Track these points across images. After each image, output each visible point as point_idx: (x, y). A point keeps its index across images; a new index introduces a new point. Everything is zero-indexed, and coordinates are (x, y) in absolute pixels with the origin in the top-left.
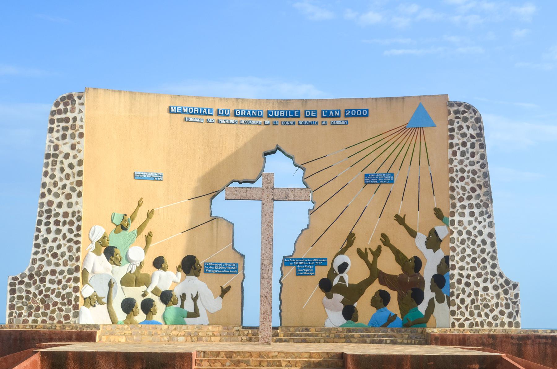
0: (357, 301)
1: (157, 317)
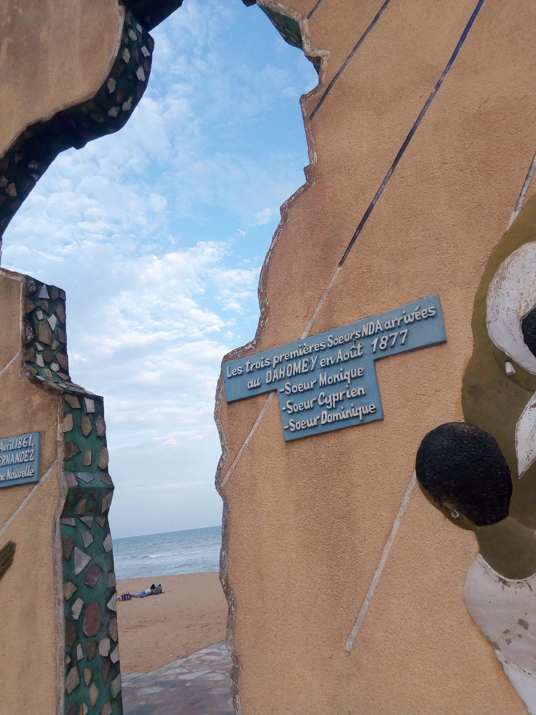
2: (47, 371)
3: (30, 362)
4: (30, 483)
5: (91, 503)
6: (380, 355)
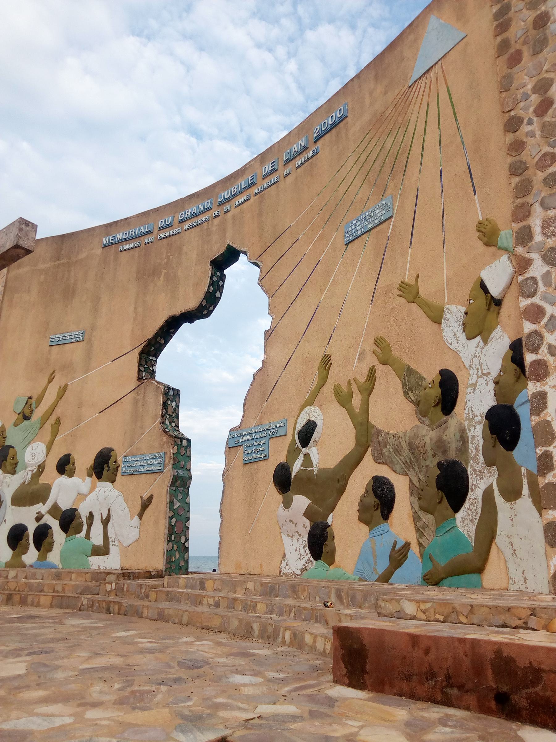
0: (332, 511)
1: (54, 557)
2: (170, 426)
3: (164, 423)
4: (160, 472)
5: (182, 482)
6: (270, 437)
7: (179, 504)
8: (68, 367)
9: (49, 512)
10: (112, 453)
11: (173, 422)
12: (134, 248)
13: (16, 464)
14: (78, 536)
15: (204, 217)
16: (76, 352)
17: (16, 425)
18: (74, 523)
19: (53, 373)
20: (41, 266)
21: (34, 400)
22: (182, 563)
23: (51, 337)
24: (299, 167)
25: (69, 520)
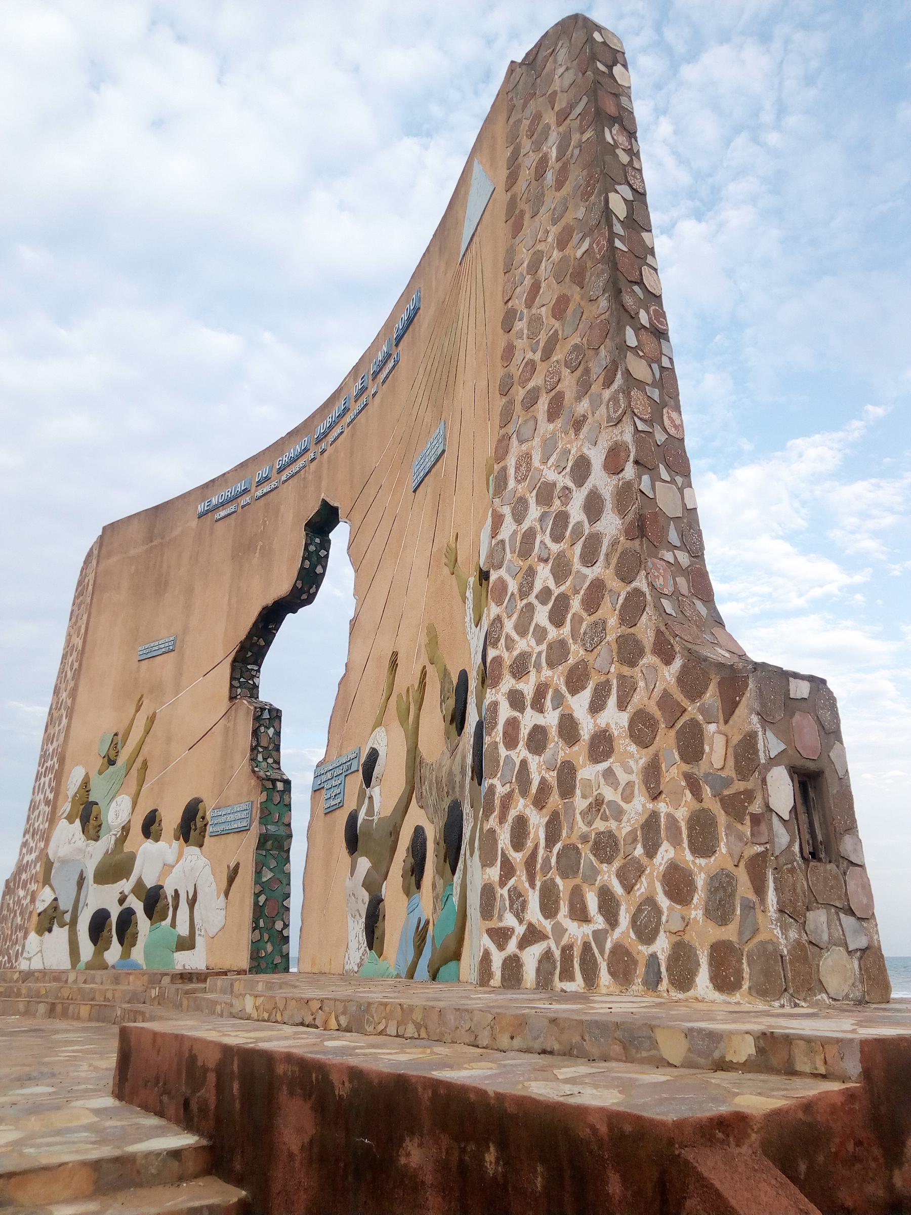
0: (385, 879)
1: (138, 954)
2: (264, 764)
5: (276, 843)
7: (272, 874)
8: (156, 689)
9: (134, 891)
10: (201, 806)
11: (270, 756)
12: (229, 515)
13: (100, 826)
14: (163, 923)
15: (300, 463)
16: (165, 666)
17: (100, 773)
18: (159, 905)
19: (140, 699)
20: (133, 552)
21: (120, 736)
22: (278, 960)
23: (140, 648)
24: (384, 382)
25: (154, 901)
